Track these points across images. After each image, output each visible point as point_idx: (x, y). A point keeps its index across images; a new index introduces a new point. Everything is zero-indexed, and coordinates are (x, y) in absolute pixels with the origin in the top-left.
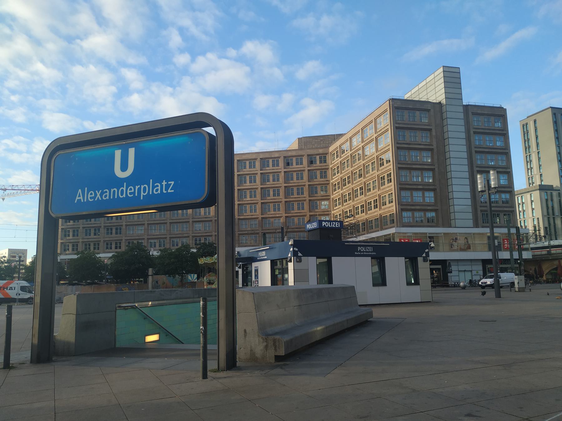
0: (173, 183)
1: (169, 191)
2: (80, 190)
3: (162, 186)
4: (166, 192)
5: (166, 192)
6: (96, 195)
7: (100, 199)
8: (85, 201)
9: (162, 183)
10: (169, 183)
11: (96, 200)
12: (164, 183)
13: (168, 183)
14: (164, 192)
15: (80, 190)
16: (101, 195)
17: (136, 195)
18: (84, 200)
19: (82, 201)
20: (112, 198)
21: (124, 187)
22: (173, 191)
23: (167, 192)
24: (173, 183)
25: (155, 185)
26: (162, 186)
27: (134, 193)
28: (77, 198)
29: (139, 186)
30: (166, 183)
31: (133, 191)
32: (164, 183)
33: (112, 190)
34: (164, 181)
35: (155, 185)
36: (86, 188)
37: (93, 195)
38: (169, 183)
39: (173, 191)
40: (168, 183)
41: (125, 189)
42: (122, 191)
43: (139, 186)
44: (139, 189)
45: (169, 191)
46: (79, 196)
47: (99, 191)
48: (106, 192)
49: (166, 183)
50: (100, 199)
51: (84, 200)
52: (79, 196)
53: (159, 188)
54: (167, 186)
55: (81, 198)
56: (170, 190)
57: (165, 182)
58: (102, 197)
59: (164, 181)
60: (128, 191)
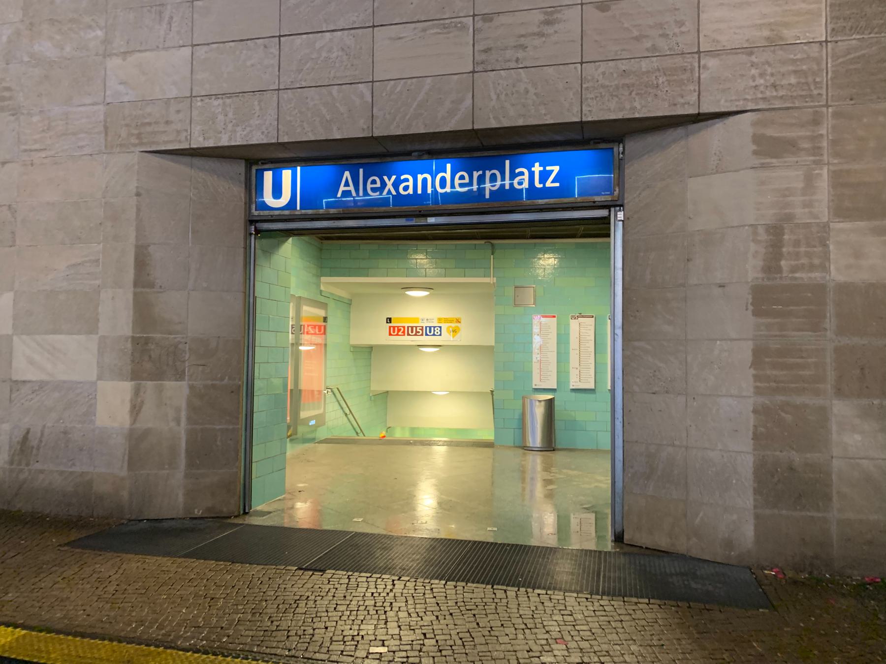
0: (556, 169)
2: (347, 174)
3: (532, 175)
4: (541, 186)
5: (541, 186)
9: (533, 169)
10: (548, 168)
12: (537, 168)
13: (545, 168)
14: (538, 185)
15: (347, 174)
20: (419, 191)
21: (446, 173)
22: (557, 185)
23: (544, 185)
24: (556, 169)
25: (517, 171)
26: (532, 175)
28: (342, 188)
29: (480, 172)
30: (542, 169)
32: (537, 168)
33: (420, 177)
34: (537, 164)
35: (517, 171)
37: (378, 185)
38: (548, 168)
39: (557, 185)
40: (545, 168)
41: (448, 176)
42: (443, 182)
43: (480, 172)
44: (481, 179)
45: (549, 184)
46: (347, 184)
48: (407, 180)
49: (542, 169)
52: (347, 184)
53: (526, 176)
54: (544, 176)
55: (351, 188)
57: (540, 166)
58: (397, 189)
59: (537, 164)
60: (457, 181)
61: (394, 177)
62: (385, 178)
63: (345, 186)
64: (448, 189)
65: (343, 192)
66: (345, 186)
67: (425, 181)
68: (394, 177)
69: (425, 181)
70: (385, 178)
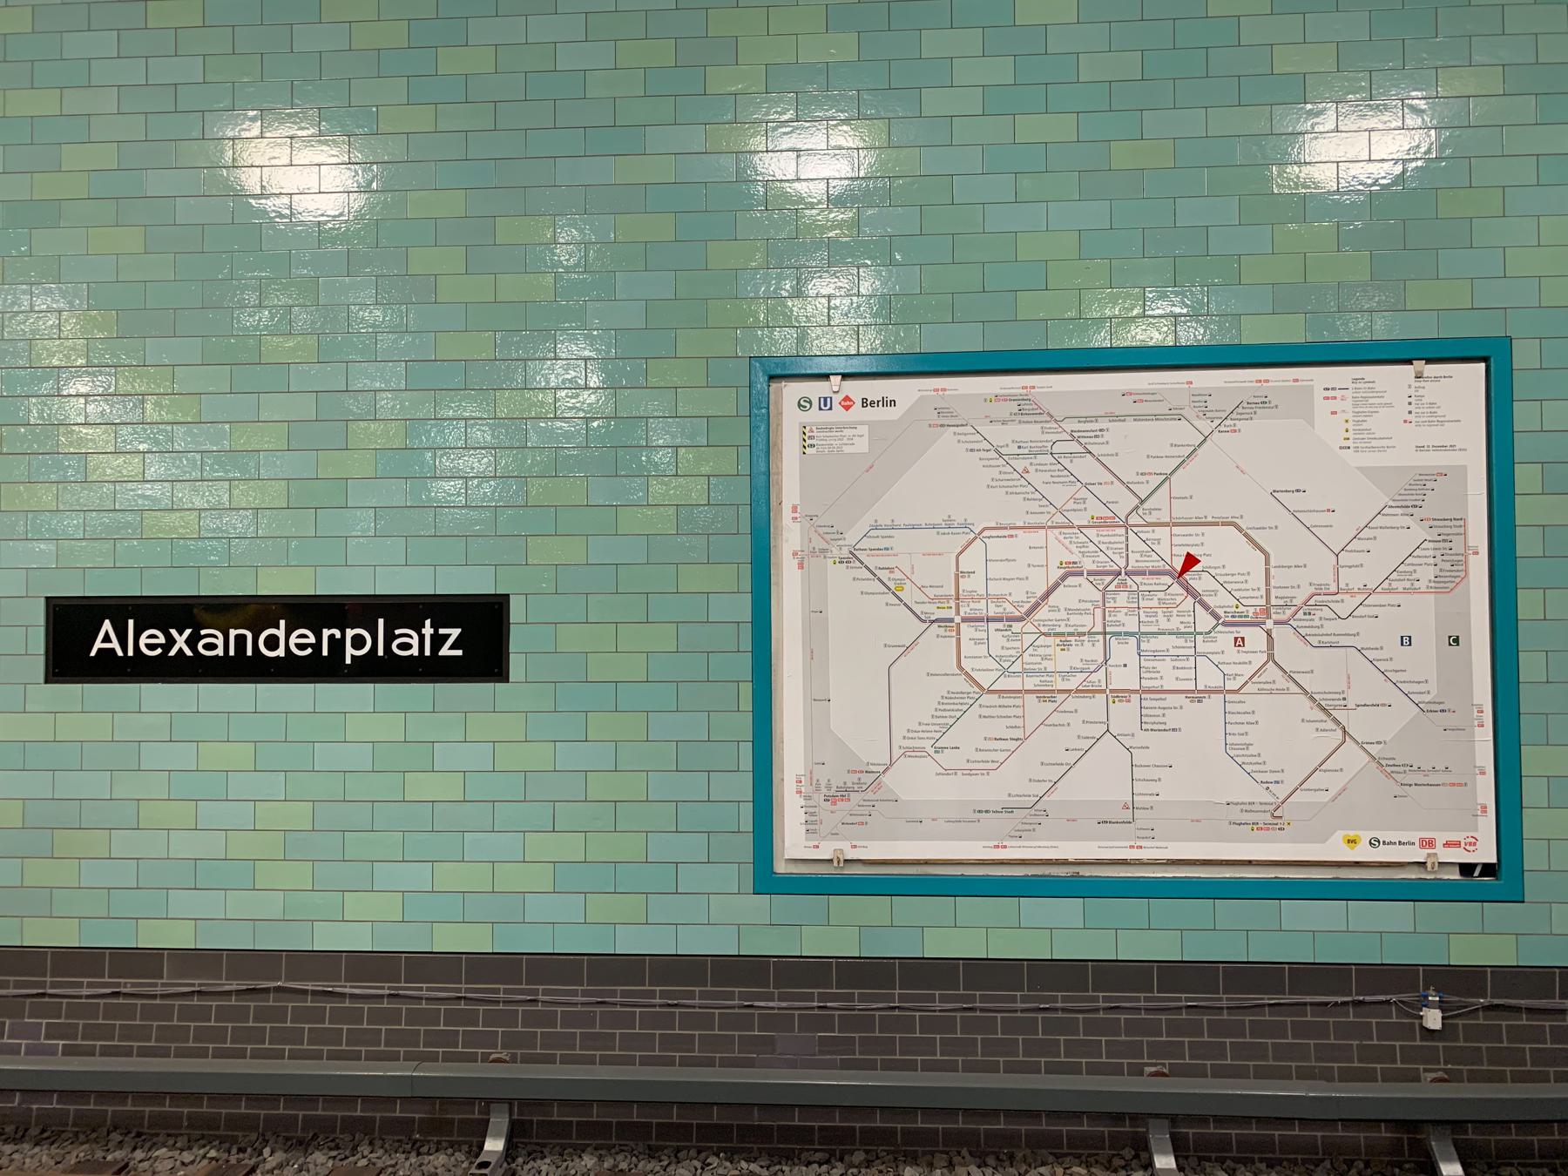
1: (445, 651)
2: (107, 625)
6: (171, 642)
7: (189, 653)
8: (130, 653)
11: (172, 653)
15: (107, 625)
16: (192, 642)
17: (325, 653)
18: (125, 649)
19: (120, 653)
22: (459, 653)
27: (317, 646)
28: (98, 645)
31: (312, 640)
32: (428, 631)
33: (233, 633)
36: (131, 622)
37: (162, 640)
39: (459, 653)
41: (281, 633)
45: (445, 651)
46: (107, 639)
47: (183, 632)
50: (189, 653)
51: (125, 649)
52: (107, 639)
54: (438, 641)
55: (115, 644)
56: (452, 648)
58: (193, 647)
61: (188, 632)
62: (173, 632)
63: (103, 641)
64: (281, 652)
65: (100, 650)
66: (103, 641)
67: (241, 640)
68: (188, 632)
69: (241, 640)
70: (173, 632)
